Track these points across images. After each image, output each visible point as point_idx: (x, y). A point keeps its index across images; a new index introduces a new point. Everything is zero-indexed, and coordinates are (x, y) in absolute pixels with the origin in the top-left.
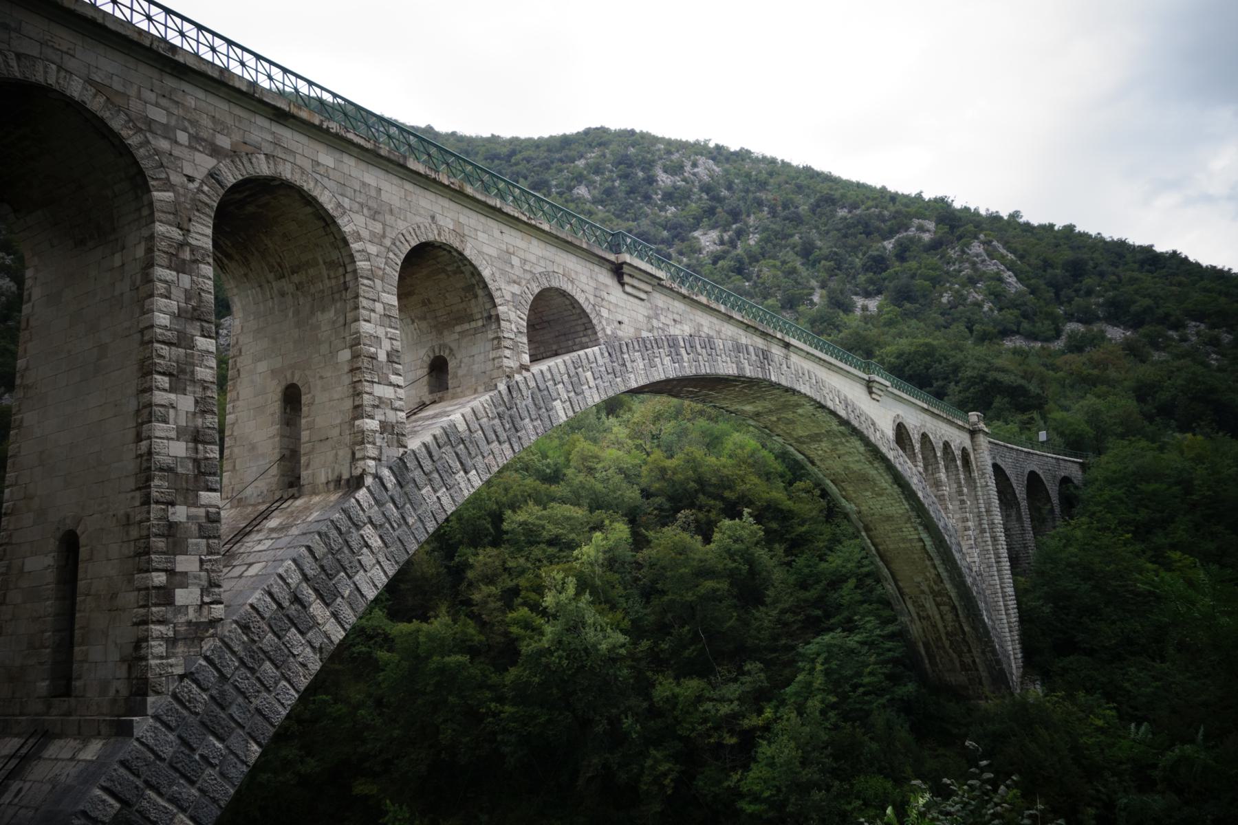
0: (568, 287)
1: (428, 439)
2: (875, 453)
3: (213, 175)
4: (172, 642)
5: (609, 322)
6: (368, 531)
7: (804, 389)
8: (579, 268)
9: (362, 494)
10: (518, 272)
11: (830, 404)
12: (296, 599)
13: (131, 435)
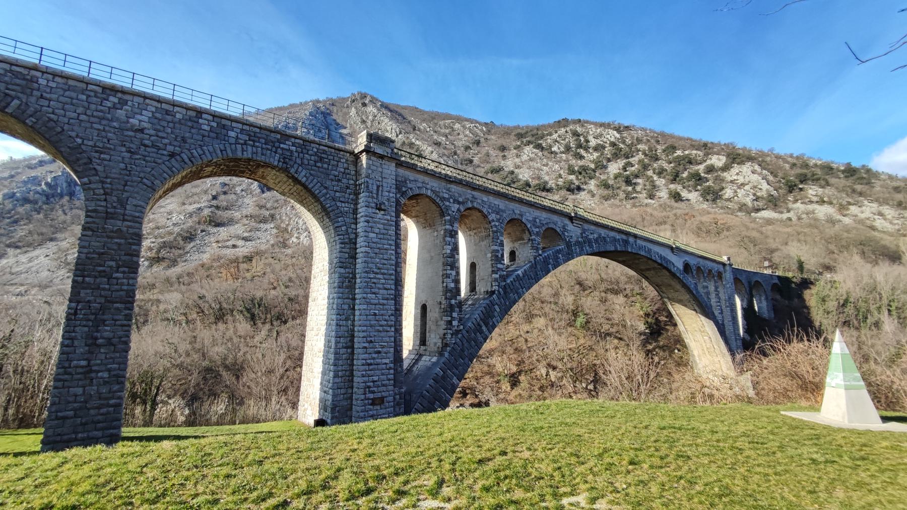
0: (554, 227)
1: (512, 280)
2: (673, 275)
3: (459, 210)
4: (452, 335)
5: (568, 237)
6: (496, 307)
7: (643, 253)
8: (558, 220)
9: (495, 296)
10: (538, 224)
11: (653, 258)
12: (479, 325)
13: (441, 281)
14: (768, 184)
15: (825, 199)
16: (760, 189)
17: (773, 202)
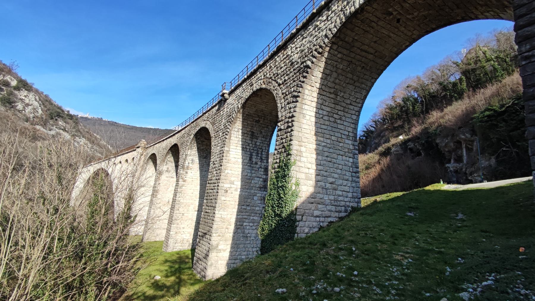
14: (42, 110)
15: (67, 129)
16: (37, 112)
17: (44, 125)
